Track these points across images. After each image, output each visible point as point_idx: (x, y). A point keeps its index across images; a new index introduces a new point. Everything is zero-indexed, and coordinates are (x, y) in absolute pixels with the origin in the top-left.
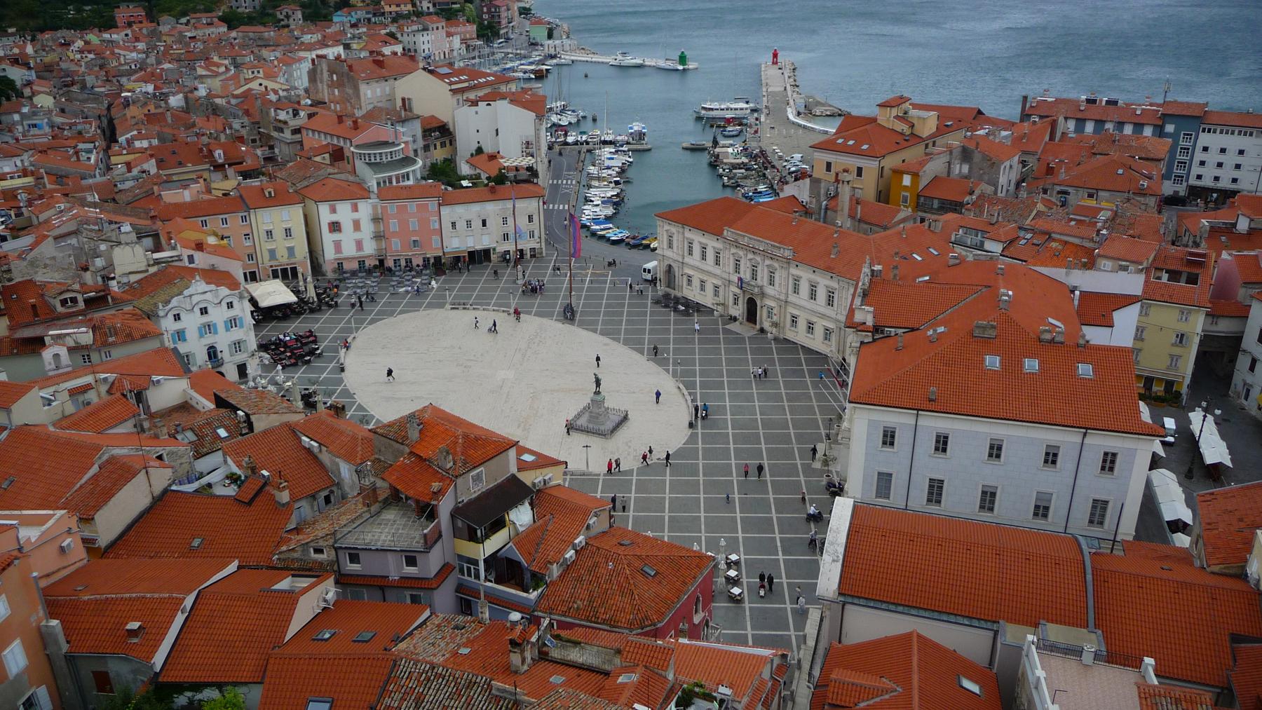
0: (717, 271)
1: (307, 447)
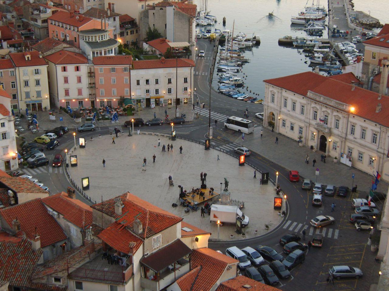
0: (302, 117)
1: (51, 214)
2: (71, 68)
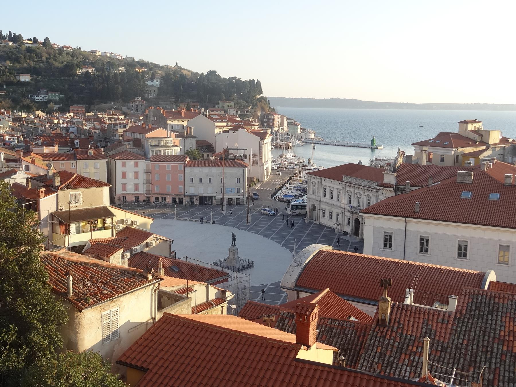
2: (131, 163)
